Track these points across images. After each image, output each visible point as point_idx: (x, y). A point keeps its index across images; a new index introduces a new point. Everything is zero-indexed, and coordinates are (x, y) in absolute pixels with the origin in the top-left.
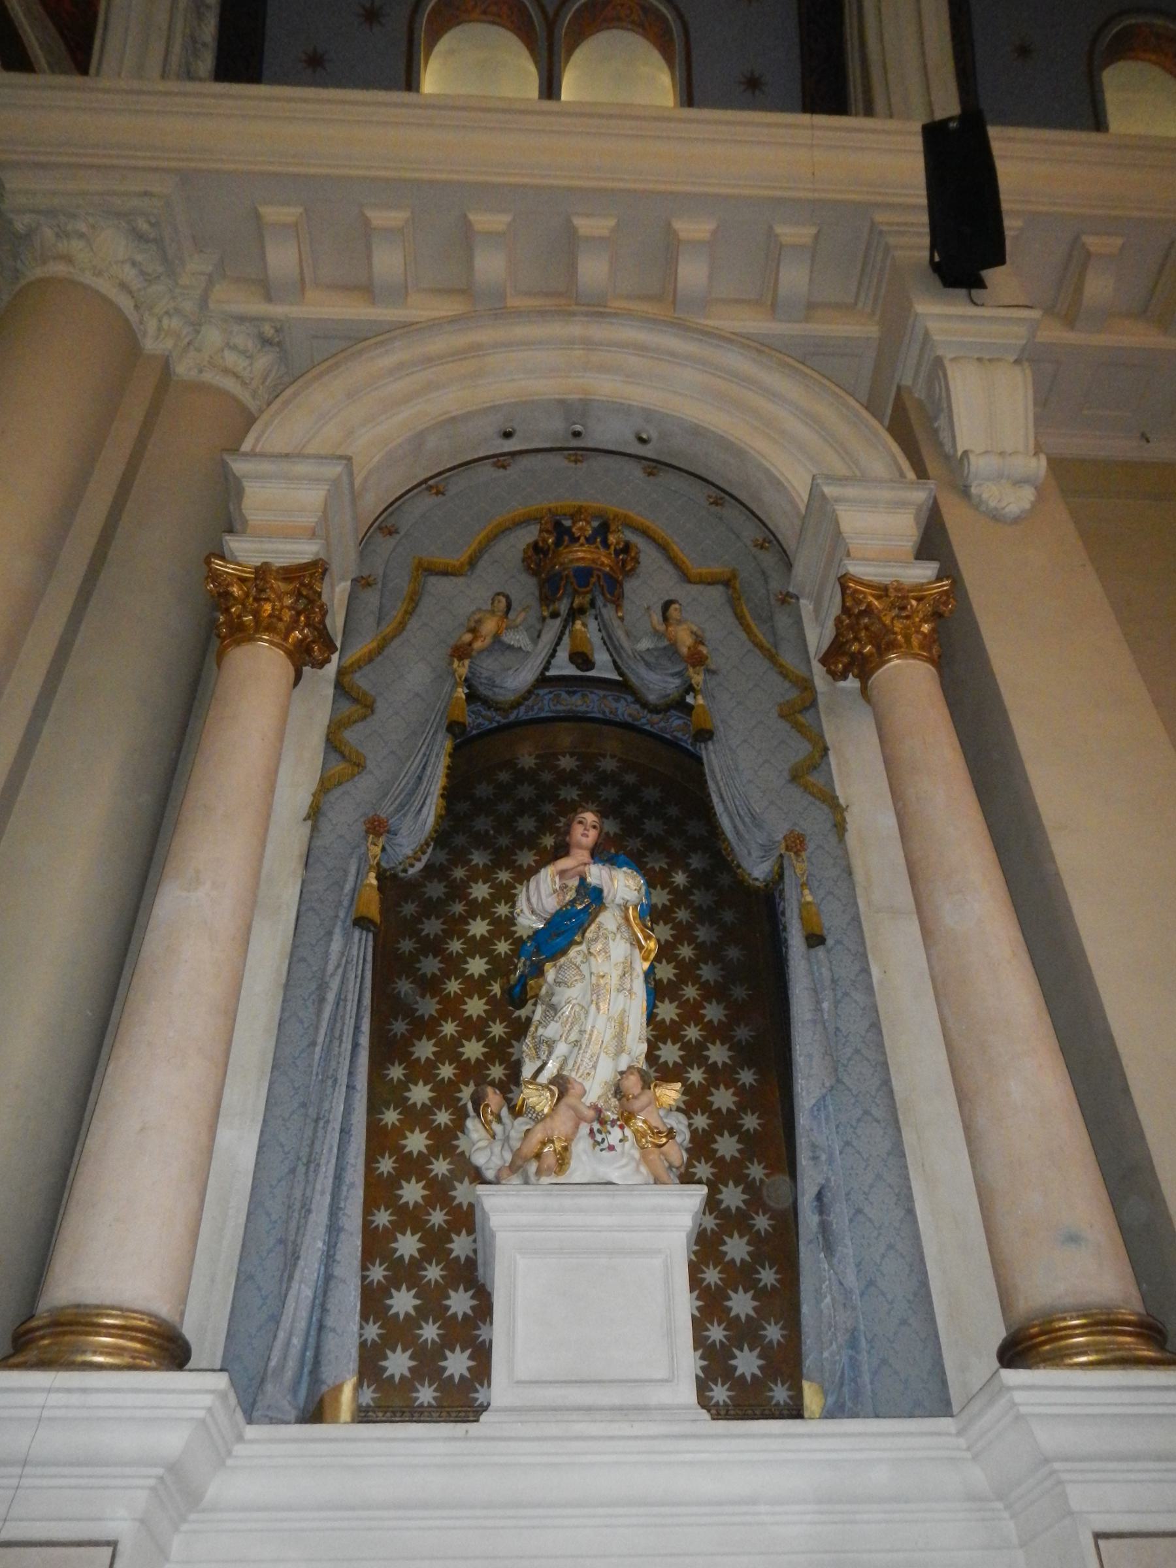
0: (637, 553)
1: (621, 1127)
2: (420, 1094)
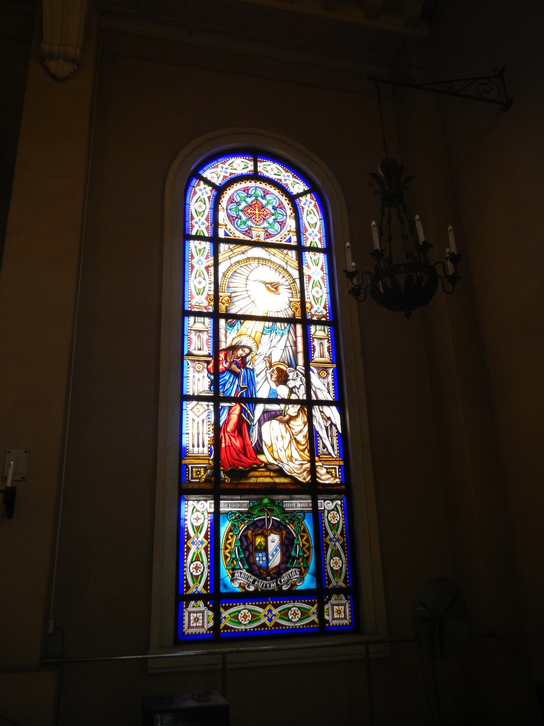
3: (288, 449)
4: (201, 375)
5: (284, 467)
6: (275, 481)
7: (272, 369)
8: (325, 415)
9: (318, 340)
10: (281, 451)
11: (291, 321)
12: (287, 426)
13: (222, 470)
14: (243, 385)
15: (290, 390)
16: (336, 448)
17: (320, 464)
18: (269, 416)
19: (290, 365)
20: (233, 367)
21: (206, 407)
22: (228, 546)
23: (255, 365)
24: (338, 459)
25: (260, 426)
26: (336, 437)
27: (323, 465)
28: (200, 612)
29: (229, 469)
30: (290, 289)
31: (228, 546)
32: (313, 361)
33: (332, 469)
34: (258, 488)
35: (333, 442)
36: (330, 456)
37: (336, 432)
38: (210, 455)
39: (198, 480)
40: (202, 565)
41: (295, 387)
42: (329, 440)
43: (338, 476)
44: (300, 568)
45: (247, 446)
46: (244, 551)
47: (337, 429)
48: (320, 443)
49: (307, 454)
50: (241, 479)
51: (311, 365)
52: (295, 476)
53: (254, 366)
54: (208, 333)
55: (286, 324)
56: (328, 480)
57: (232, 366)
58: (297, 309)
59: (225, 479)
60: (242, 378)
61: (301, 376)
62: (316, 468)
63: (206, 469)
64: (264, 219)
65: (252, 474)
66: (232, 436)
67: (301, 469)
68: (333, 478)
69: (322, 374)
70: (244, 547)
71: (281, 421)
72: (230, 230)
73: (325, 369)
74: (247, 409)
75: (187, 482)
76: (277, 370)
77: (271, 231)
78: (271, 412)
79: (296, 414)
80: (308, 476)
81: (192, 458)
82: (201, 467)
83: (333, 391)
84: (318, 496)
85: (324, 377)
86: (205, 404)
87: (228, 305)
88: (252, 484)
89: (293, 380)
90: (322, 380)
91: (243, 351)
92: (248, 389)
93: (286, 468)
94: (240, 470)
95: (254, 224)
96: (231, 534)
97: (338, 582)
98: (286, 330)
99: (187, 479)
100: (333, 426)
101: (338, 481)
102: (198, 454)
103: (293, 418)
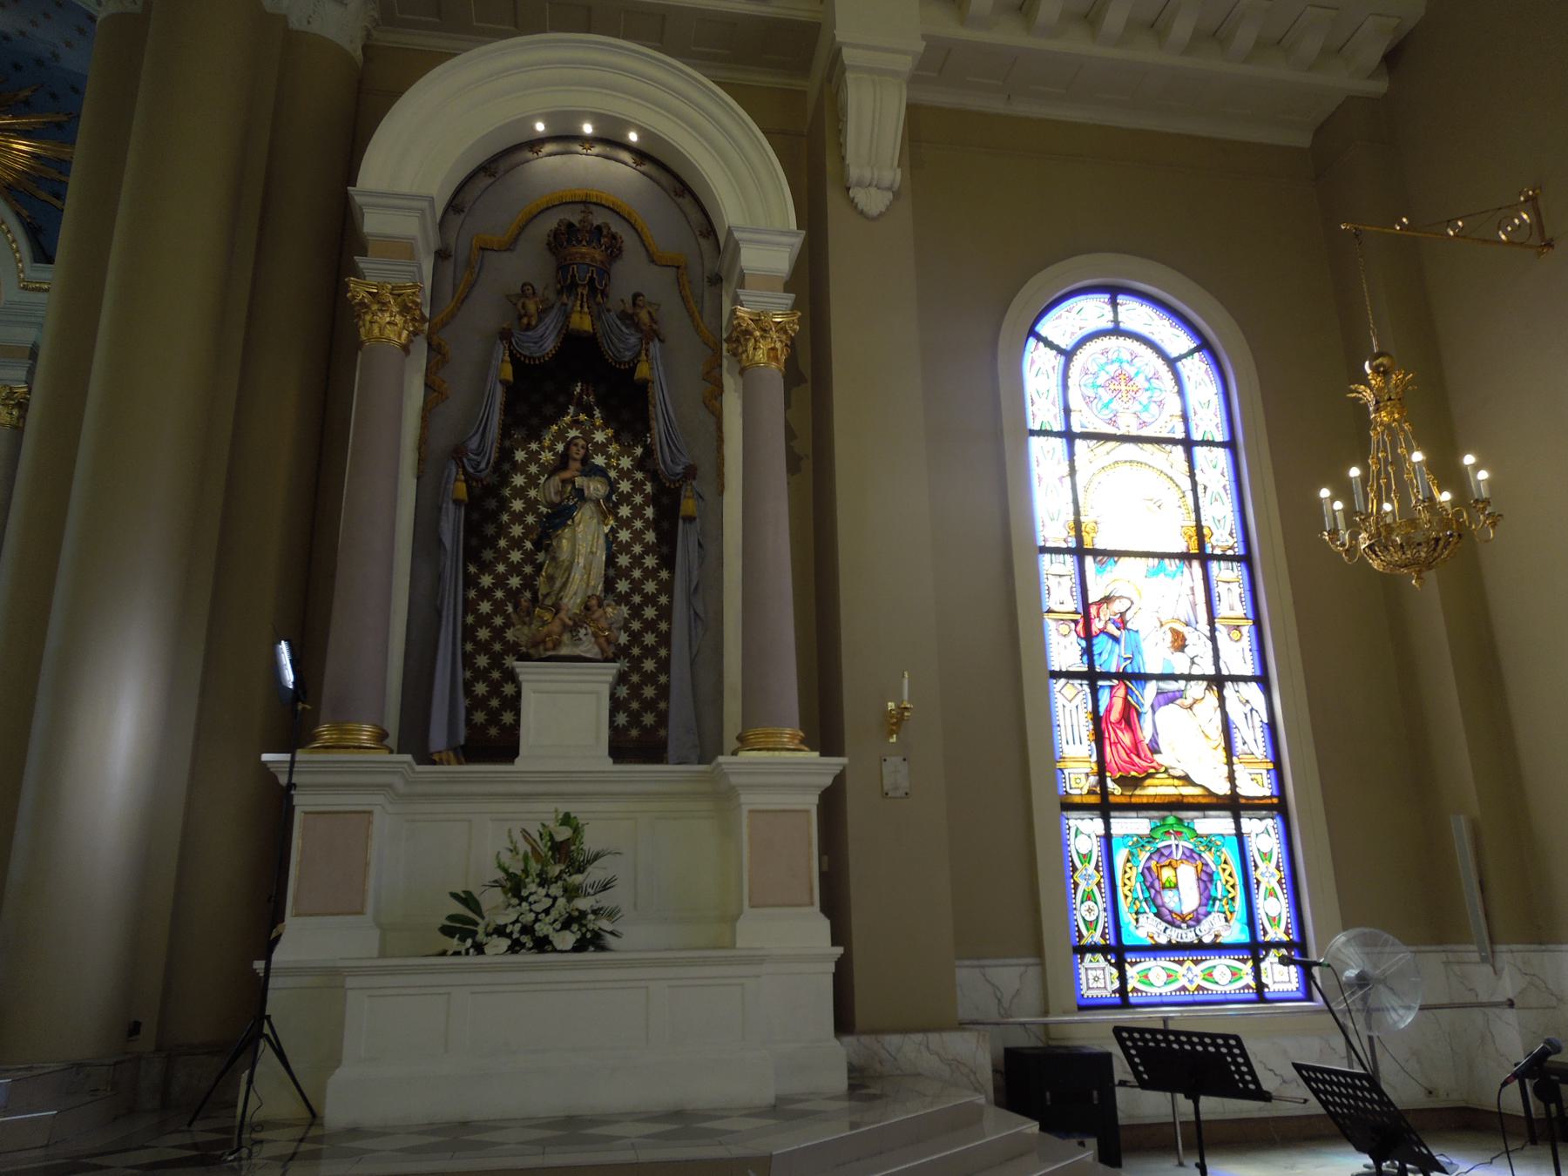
0: (622, 242)
1: (586, 628)
2: (486, 581)
11: (1185, 557)
16: (1261, 744)
18: (1169, 698)
21: (1079, 687)
22: (1127, 882)
25: (1154, 712)
28: (1099, 968)
29: (1118, 776)
31: (1127, 882)
34: (1159, 801)
40: (1095, 906)
44: (1224, 913)
46: (1148, 888)
50: (1135, 789)
55: (1177, 561)
58: (1190, 537)
64: (1134, 398)
65: (1148, 782)
70: (1148, 884)
73: (1237, 628)
77: (1145, 417)
82: (1081, 774)
84: (1242, 812)
86: (1077, 682)
92: (1131, 659)
96: (1129, 865)
97: (1276, 933)
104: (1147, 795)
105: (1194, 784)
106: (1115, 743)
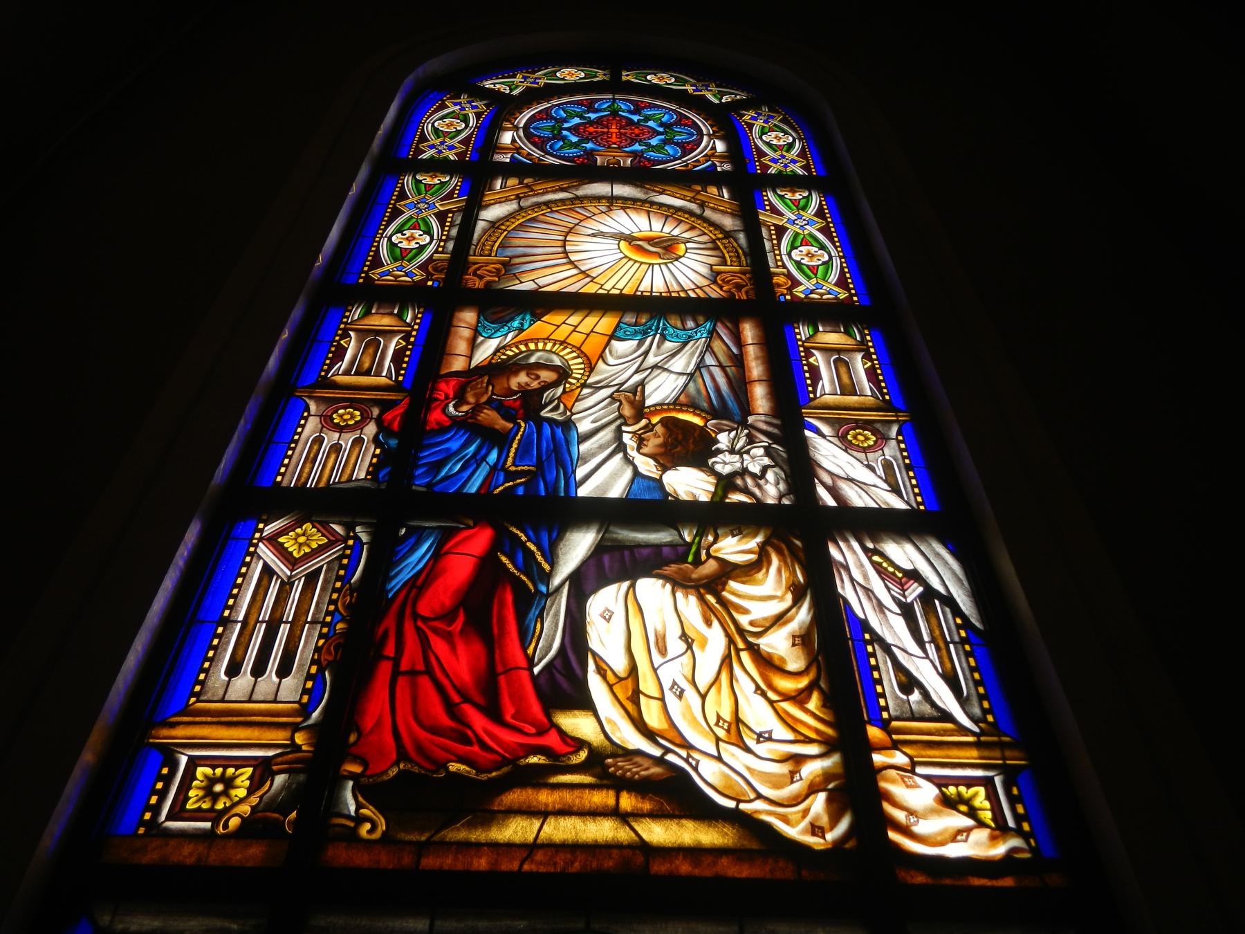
3: (719, 691)
4: (347, 441)
5: (695, 769)
6: (645, 836)
7: (644, 422)
8: (892, 563)
9: (829, 354)
10: (680, 697)
12: (710, 598)
13: (353, 776)
14: (517, 466)
15: (723, 482)
17: (899, 758)
19: (718, 412)
20: (487, 417)
23: (574, 410)
24: (995, 739)
26: (959, 646)
27: (914, 764)
29: (393, 772)
30: (716, 248)
32: (812, 404)
33: (969, 786)
35: (948, 665)
36: (949, 726)
37: (958, 627)
38: (305, 710)
39: (208, 825)
41: (744, 472)
42: (927, 657)
43: (1011, 823)
45: (505, 672)
47: (957, 612)
48: (881, 666)
49: (821, 715)
50: (449, 823)
51: (807, 413)
52: (757, 812)
53: (573, 414)
54: (406, 338)
56: (954, 839)
57: (482, 415)
59: (360, 819)
60: (515, 446)
61: (765, 441)
62: (879, 777)
63: (263, 770)
65: (515, 797)
66: (435, 631)
67: (792, 782)
68: (983, 834)
69: (855, 437)
71: (679, 583)
72: (529, 154)
74: (524, 538)
75: (141, 831)
76: (663, 425)
78: (635, 550)
79: (753, 557)
80: (834, 821)
81: (209, 719)
82: (240, 763)
83: (913, 487)
85: (866, 445)
87: (497, 279)
88: (510, 846)
89: (732, 451)
90: (861, 456)
91: (533, 377)
93: (708, 774)
94: (457, 775)
95: (604, 146)
98: (700, 329)
99: (147, 816)
100: (937, 602)
101: (1013, 850)
102: (250, 701)
103: (737, 572)
104: (495, 846)
105: (699, 808)
106: (413, 673)
